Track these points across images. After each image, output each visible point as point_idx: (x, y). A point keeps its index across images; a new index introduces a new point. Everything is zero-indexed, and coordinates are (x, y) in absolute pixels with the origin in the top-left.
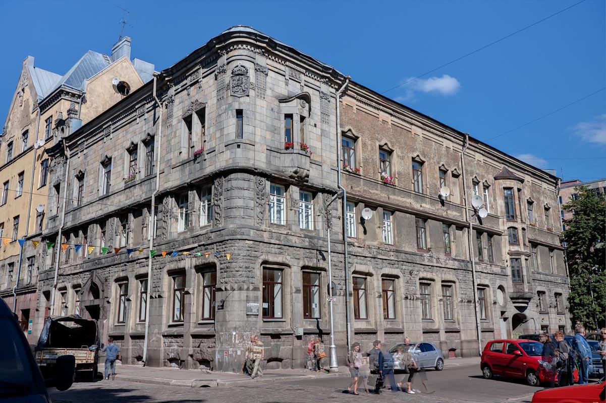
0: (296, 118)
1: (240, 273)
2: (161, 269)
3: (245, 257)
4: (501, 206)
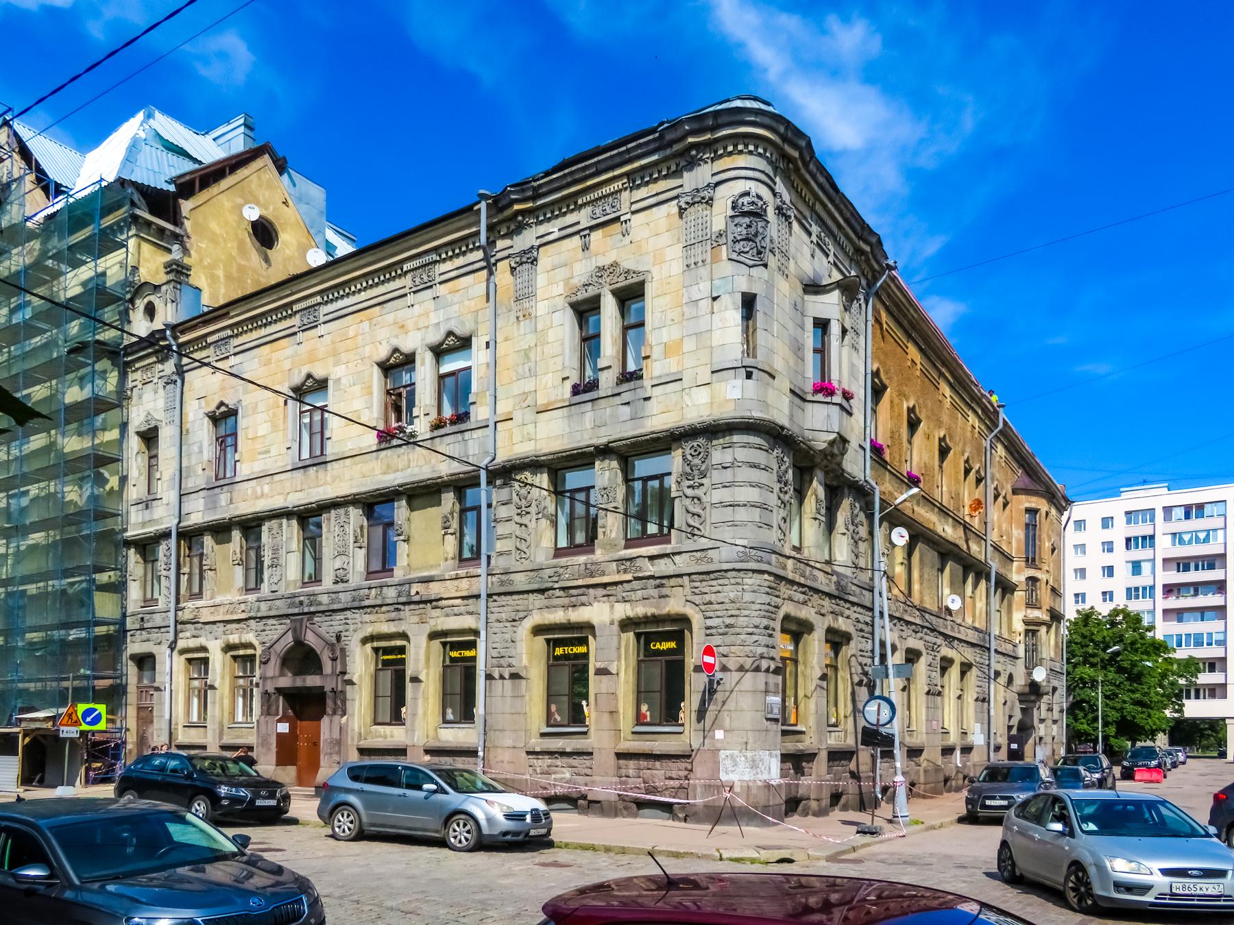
0: (835, 329)
1: (755, 638)
2: (514, 621)
3: (764, 607)
4: (1018, 541)
